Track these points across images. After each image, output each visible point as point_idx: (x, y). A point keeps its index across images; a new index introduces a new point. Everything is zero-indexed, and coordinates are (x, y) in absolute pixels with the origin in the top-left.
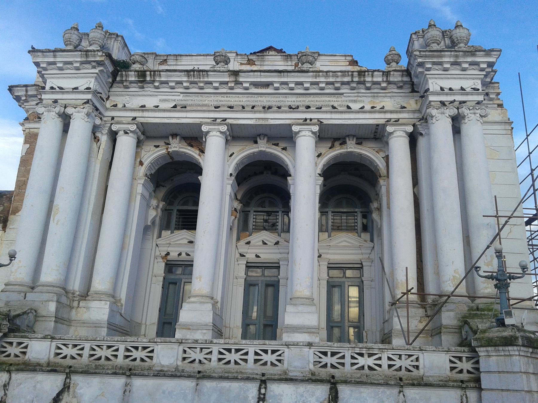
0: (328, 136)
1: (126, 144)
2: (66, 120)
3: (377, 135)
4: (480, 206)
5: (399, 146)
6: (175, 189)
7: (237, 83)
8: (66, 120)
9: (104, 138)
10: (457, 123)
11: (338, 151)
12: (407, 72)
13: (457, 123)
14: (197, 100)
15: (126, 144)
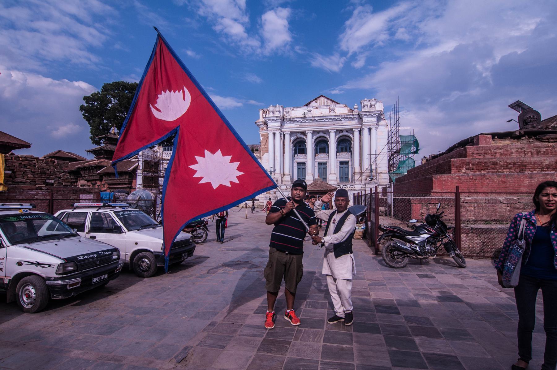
0: (338, 131)
1: (287, 137)
2: (274, 134)
3: (351, 131)
4: (373, 152)
5: (356, 134)
6: (299, 146)
7: (315, 120)
8: (274, 134)
9: (282, 136)
10: (370, 129)
11: (341, 134)
12: (358, 115)
13: (370, 129)
14: (304, 124)
15: (287, 137)
